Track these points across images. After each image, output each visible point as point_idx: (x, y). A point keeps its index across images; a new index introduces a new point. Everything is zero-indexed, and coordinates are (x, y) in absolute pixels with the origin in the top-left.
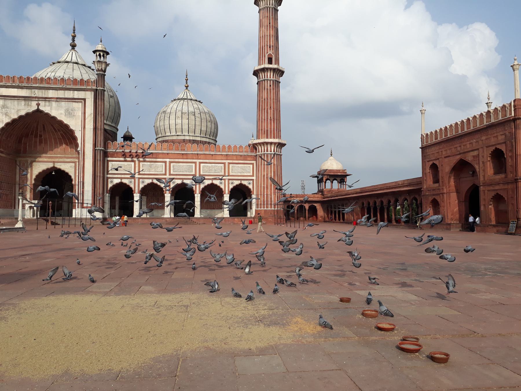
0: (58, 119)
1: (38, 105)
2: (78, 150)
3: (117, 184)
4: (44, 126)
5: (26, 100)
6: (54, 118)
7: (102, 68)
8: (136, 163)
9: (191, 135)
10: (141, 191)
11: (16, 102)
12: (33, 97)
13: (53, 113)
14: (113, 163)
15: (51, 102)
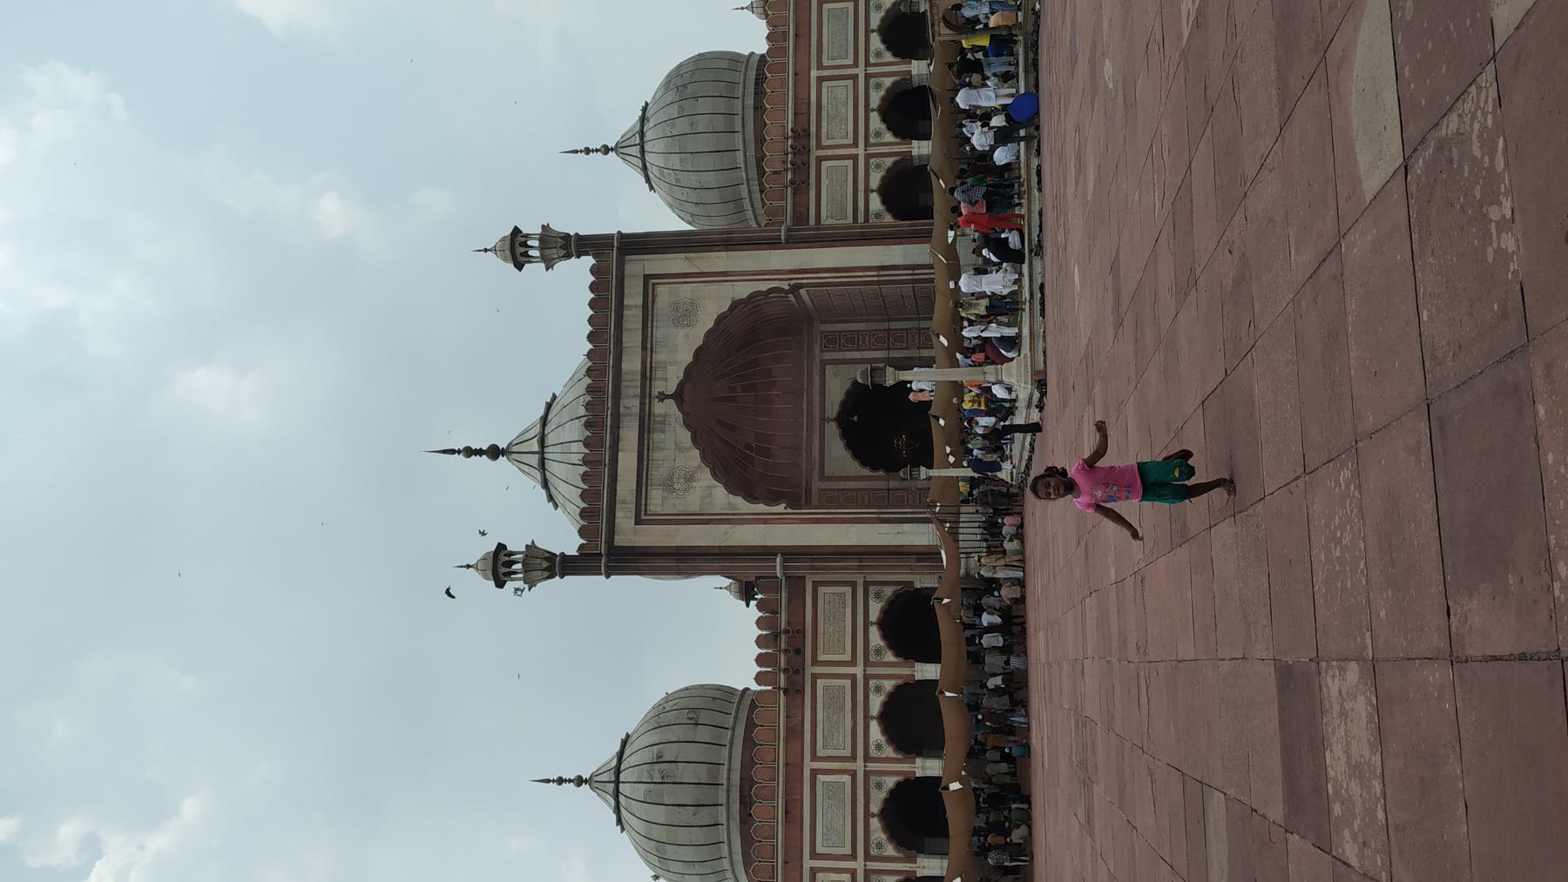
0: (701, 343)
1: (663, 397)
2: (788, 288)
3: (884, 202)
4: (719, 421)
5: (649, 428)
6: (698, 354)
7: (560, 238)
8: (824, 154)
9: (741, 90)
10: (902, 138)
11: (656, 455)
12: (642, 409)
13: (686, 357)
14: (824, 214)
15: (654, 365)
